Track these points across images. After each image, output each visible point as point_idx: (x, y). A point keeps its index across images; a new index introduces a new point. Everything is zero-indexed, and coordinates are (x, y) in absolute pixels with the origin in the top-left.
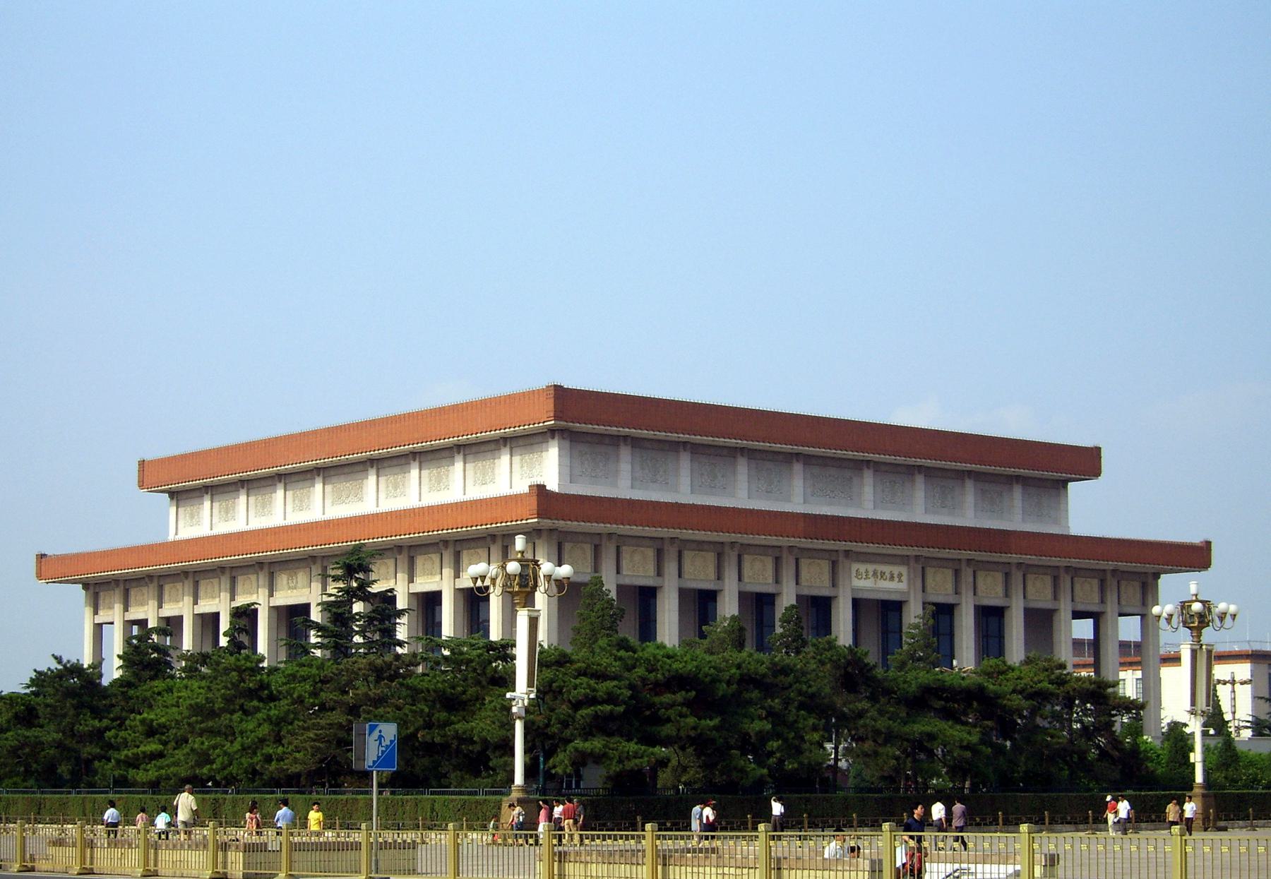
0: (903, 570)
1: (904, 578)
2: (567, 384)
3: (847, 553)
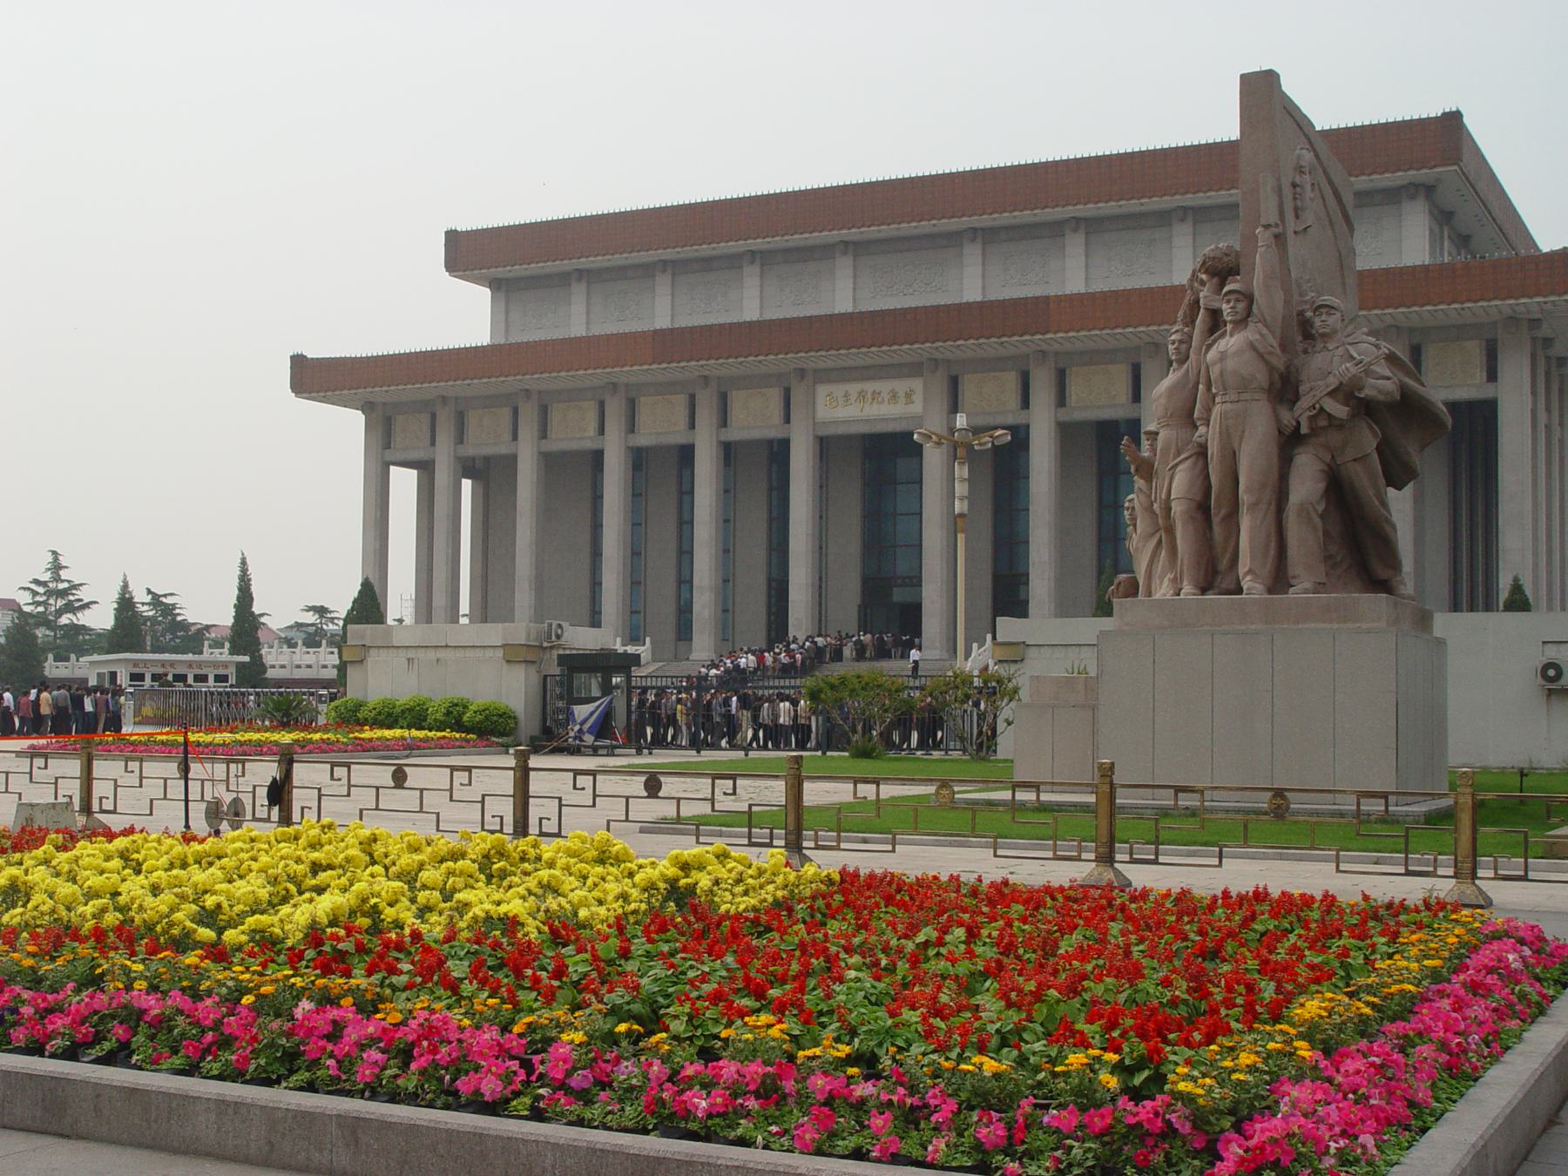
0: (917, 384)
1: (918, 398)
2: (461, 227)
3: (802, 373)
